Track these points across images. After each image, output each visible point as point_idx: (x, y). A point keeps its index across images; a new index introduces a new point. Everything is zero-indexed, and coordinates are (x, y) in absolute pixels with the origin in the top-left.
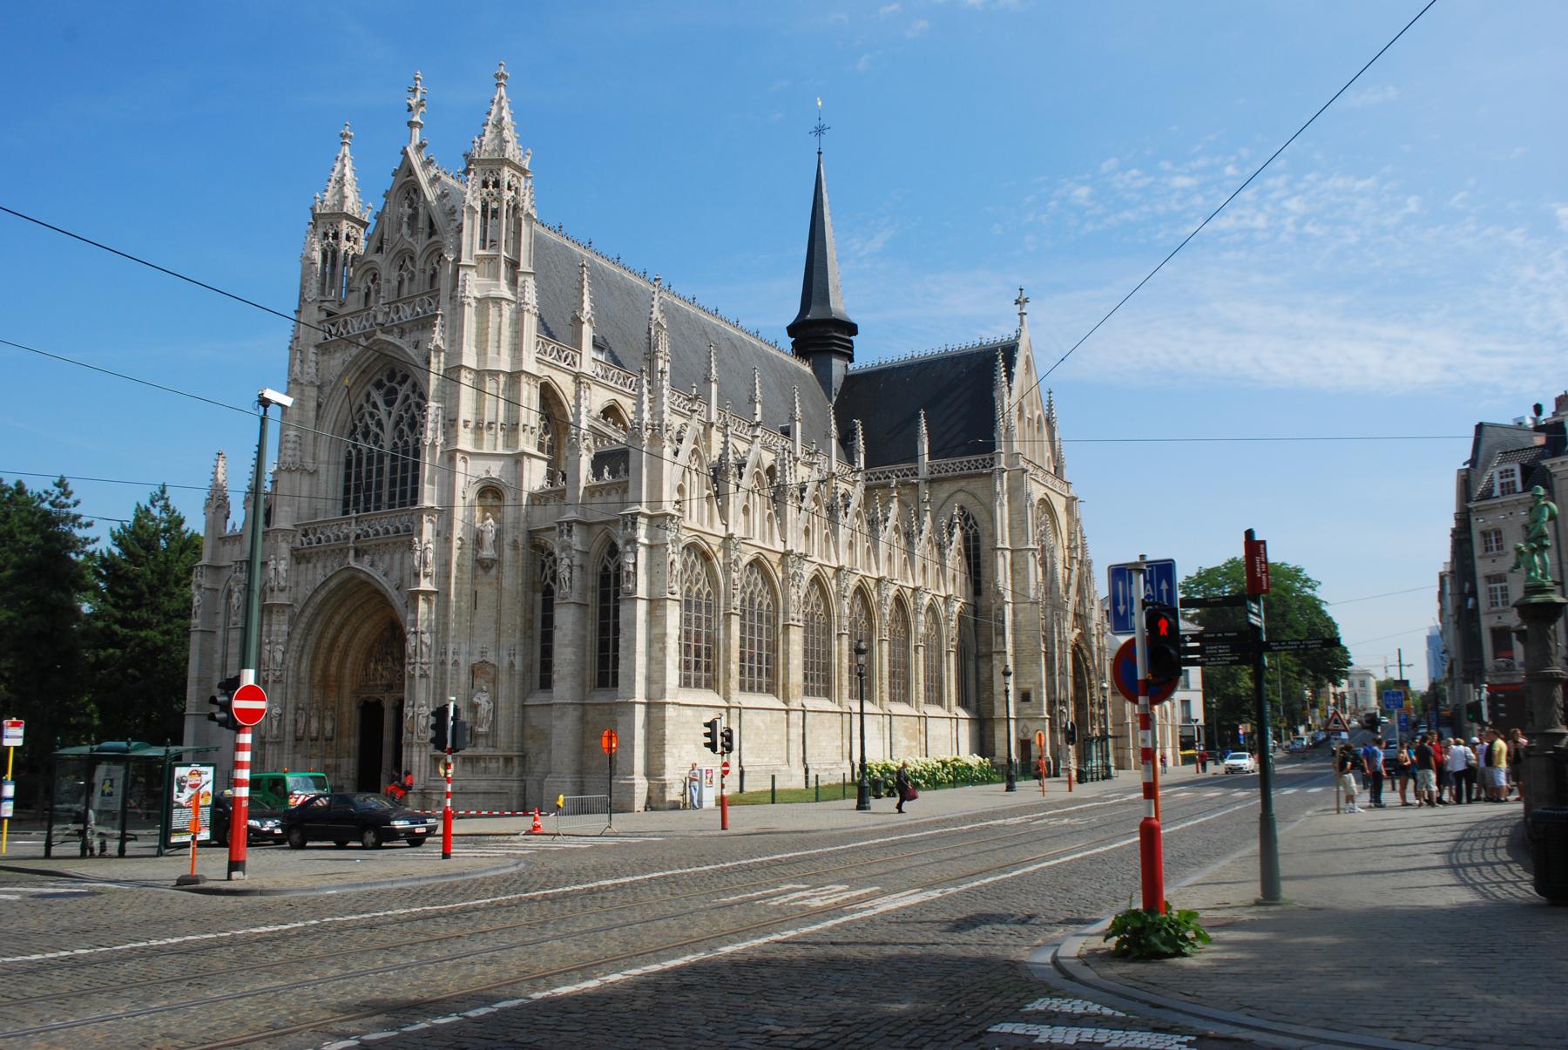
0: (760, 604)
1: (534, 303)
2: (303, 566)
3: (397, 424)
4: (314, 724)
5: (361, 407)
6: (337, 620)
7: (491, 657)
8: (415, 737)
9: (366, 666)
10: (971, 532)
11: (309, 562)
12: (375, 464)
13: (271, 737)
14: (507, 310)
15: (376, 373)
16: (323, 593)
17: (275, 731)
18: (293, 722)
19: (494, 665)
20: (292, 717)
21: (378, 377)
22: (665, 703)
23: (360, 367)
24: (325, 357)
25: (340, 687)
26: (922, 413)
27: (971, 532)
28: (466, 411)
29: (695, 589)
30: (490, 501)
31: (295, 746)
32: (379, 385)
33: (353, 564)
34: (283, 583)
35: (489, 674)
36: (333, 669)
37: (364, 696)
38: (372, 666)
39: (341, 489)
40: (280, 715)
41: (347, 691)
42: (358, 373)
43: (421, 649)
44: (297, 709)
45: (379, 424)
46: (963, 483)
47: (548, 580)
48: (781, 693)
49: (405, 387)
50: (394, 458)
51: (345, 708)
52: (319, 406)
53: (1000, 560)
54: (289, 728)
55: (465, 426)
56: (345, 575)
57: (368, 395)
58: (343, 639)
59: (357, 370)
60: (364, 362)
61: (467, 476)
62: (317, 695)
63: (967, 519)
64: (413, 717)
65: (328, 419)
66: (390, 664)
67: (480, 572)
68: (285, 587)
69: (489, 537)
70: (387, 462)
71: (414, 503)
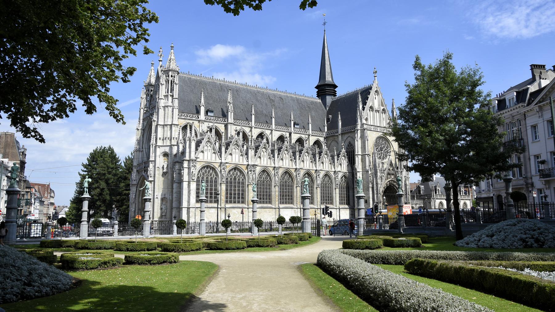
0: (239, 179)
1: (177, 106)
10: (352, 150)
14: (170, 109)
17: (133, 215)
22: (190, 208)
26: (339, 113)
27: (352, 150)
28: (160, 135)
29: (209, 178)
46: (350, 134)
48: (247, 203)
53: (357, 159)
55: (160, 139)
61: (159, 151)
63: (351, 146)
69: (165, 166)
71: (149, 159)
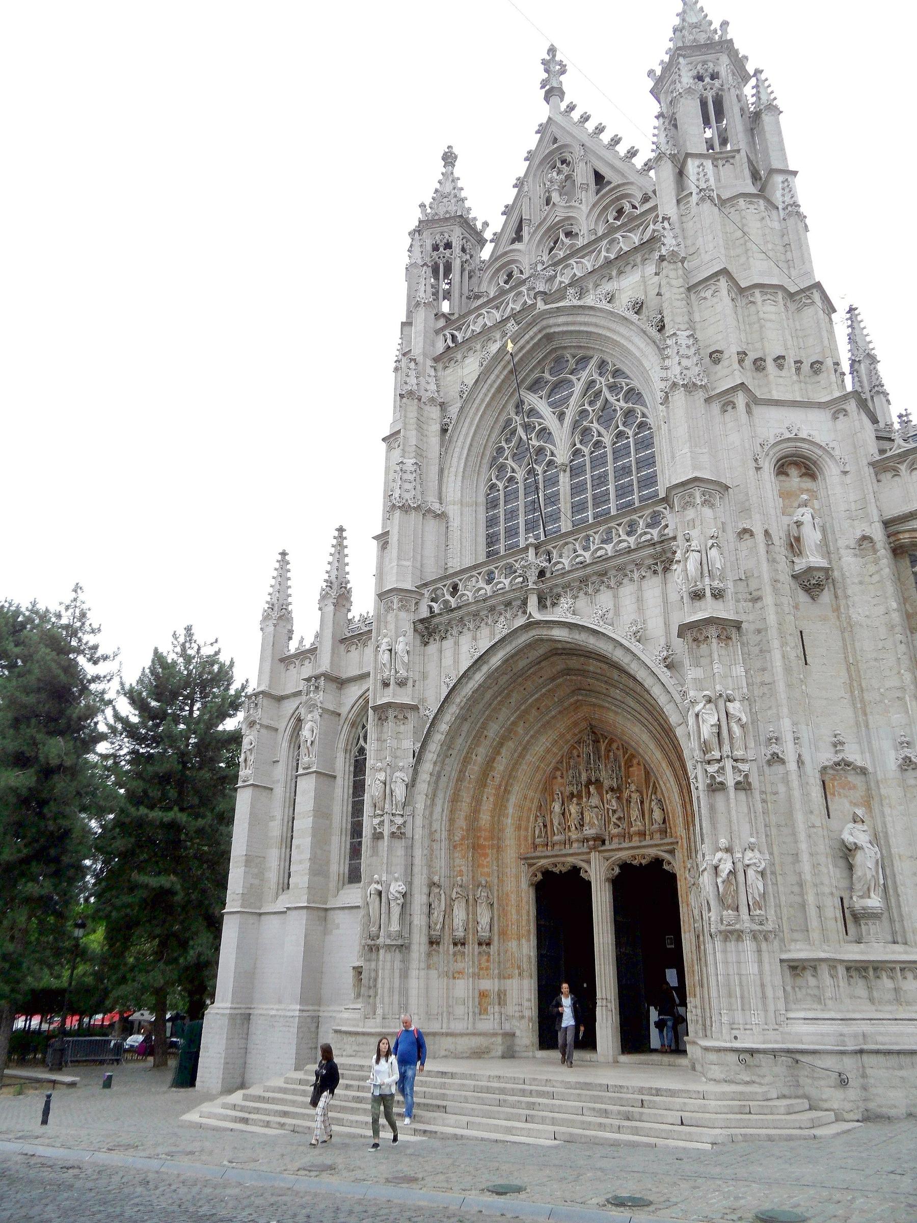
2: (433, 648)
3: (575, 424)
4: (460, 914)
5: (509, 421)
6: (493, 730)
7: (853, 754)
8: (744, 915)
9: (543, 809)
11: (443, 639)
12: (502, 541)
13: (389, 936)
15: (532, 371)
16: (479, 677)
17: (395, 927)
18: (425, 909)
19: (863, 771)
20: (424, 899)
21: (535, 375)
24: (448, 371)
25: (499, 849)
30: (795, 479)
31: (429, 955)
32: (534, 387)
33: (538, 616)
34: (403, 673)
35: (855, 787)
36: (485, 818)
37: (543, 862)
38: (557, 807)
39: (482, 540)
40: (404, 895)
41: (510, 854)
43: (729, 730)
44: (432, 884)
45: (544, 433)
49: (584, 375)
51: (510, 885)
52: (444, 431)
54: (419, 919)
56: (523, 639)
57: (519, 405)
58: (501, 765)
59: (504, 367)
62: (461, 863)
64: (733, 873)
65: (459, 443)
66: (595, 801)
67: (803, 597)
68: (407, 679)
70: (564, 480)
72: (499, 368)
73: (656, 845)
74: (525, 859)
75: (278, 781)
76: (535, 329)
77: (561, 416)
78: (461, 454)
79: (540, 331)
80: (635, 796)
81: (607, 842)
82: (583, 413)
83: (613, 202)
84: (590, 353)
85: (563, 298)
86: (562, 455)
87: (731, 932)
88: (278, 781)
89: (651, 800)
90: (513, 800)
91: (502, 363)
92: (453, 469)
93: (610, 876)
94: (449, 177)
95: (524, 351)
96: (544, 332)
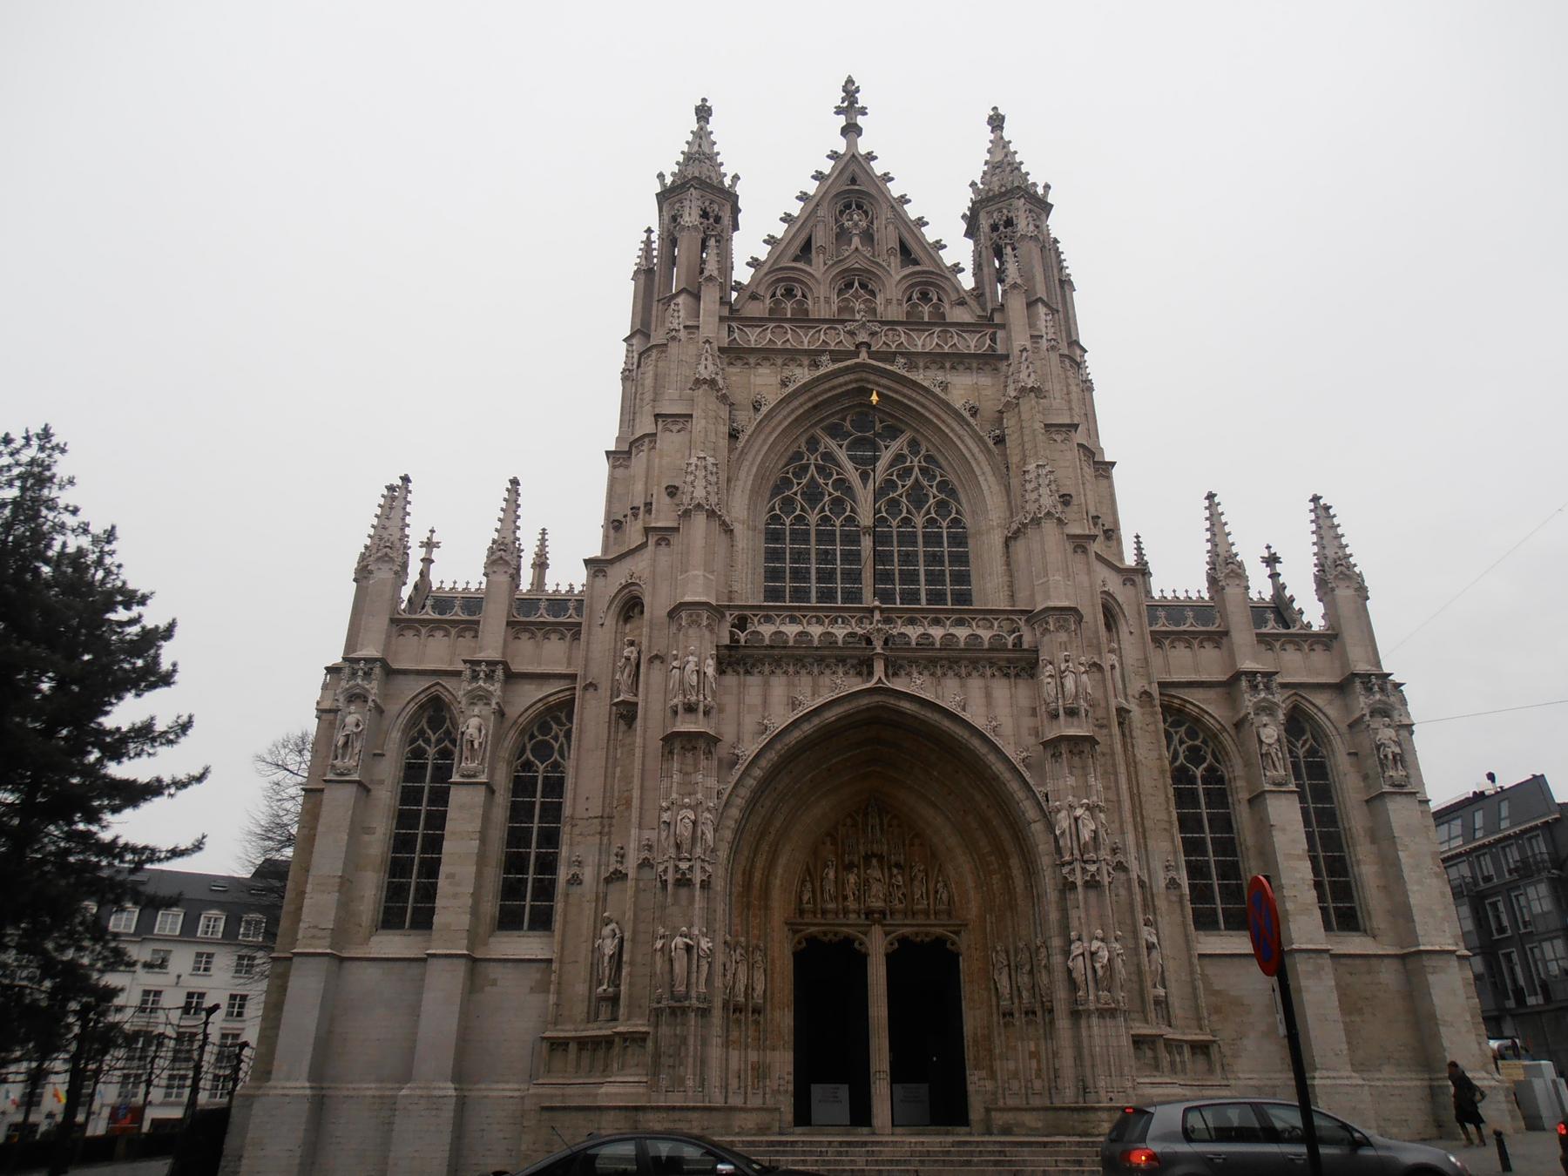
5: (798, 456)
15: (832, 414)
21: (835, 420)
23: (816, 396)
37: (812, 929)
42: (810, 405)
47: (1181, 759)
50: (880, 539)
59: (811, 399)
60: (826, 391)
72: (805, 397)
73: (943, 925)
74: (792, 924)
75: (382, 782)
76: (852, 377)
77: (864, 477)
78: (749, 470)
79: (856, 381)
80: (921, 875)
81: (888, 917)
82: (890, 485)
83: (926, 283)
84: (903, 427)
85: (892, 362)
86: (866, 518)
87: (1106, 1010)
88: (382, 782)
89: (937, 882)
90: (782, 860)
91: (810, 394)
92: (740, 483)
93: (890, 951)
94: (701, 135)
95: (834, 393)
96: (861, 384)
